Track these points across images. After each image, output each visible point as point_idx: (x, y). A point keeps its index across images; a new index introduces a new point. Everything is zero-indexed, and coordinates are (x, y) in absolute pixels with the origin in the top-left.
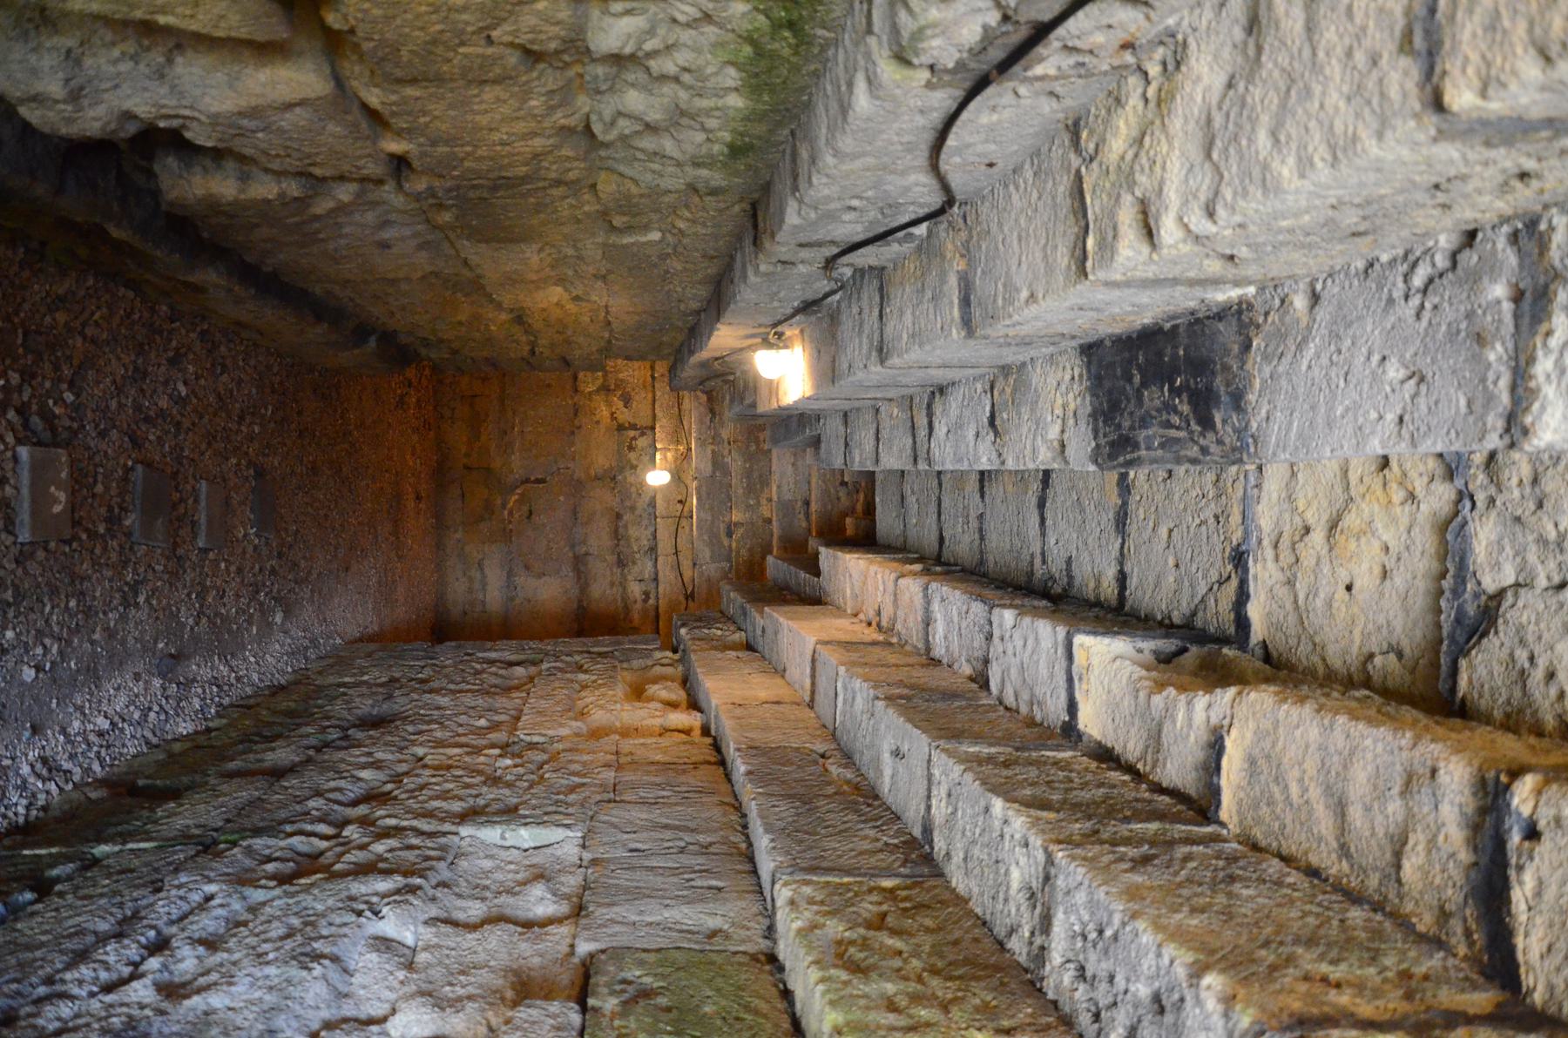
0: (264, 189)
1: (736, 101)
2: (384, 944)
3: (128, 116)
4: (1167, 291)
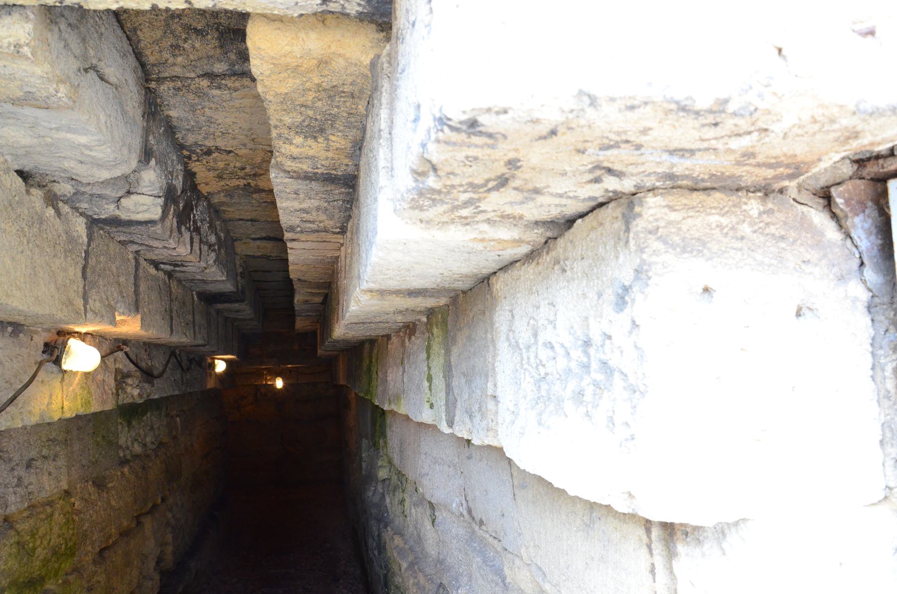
0: (169, 537)
1: (149, 414)
2: (373, 495)
3: (155, 569)
4: (197, 317)
